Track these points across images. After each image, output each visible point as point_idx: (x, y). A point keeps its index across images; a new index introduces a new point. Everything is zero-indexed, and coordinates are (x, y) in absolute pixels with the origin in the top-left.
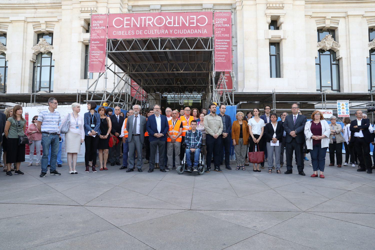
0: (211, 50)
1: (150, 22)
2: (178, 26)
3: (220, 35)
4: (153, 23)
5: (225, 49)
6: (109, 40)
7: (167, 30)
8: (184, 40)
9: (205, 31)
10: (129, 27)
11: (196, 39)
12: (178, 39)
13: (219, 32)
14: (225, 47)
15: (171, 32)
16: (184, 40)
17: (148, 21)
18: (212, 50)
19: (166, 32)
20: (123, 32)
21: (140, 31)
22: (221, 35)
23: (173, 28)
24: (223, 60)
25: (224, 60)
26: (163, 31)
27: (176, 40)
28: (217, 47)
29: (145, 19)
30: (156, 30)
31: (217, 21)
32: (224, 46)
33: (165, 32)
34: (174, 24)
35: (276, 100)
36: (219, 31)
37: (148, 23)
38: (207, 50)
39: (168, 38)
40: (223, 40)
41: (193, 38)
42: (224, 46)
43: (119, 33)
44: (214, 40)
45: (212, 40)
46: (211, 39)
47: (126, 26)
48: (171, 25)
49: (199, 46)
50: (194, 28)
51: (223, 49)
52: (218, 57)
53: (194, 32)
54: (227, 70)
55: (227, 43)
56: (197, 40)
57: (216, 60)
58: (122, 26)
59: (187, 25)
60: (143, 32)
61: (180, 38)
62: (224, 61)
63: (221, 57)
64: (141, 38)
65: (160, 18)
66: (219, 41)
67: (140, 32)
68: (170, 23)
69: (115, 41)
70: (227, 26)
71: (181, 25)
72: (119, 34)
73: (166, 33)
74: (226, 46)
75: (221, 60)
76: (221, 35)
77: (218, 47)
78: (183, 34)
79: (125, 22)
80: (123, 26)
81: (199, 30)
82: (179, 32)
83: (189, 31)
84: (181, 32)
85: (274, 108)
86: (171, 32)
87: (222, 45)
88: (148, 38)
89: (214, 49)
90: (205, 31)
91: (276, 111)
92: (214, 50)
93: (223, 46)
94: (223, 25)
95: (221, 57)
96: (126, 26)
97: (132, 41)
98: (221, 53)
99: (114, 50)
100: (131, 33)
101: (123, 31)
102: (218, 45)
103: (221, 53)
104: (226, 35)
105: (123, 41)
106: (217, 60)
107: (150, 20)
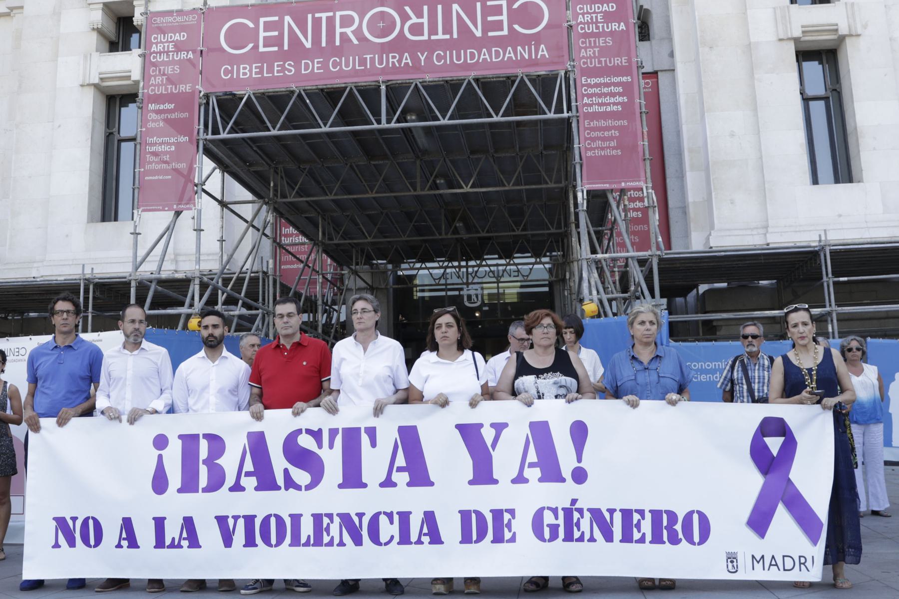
0: (565, 115)
1: (349, 31)
2: (448, 37)
3: (595, 63)
4: (358, 33)
5: (615, 108)
6: (207, 96)
7: (406, 54)
8: (469, 83)
9: (543, 51)
10: (276, 49)
11: (510, 80)
12: (447, 81)
13: (590, 52)
14: (614, 104)
15: (423, 59)
16: (469, 83)
17: (341, 27)
18: (570, 114)
19: (404, 61)
20: (256, 68)
21: (316, 61)
22: (600, 62)
23: (430, 46)
24: (609, 147)
25: (614, 148)
26: (393, 59)
27: (442, 86)
28: (586, 105)
29: (331, 21)
30: (368, 57)
31: (583, 14)
32: (612, 100)
33: (400, 61)
34: (433, 30)
35: (836, 274)
36: (590, 47)
37: (342, 34)
38: (551, 115)
39: (411, 81)
40: (607, 80)
41: (499, 77)
42: (612, 100)
43: (242, 71)
44: (575, 80)
45: (567, 79)
46: (565, 77)
47: (265, 46)
48: (422, 35)
49: (522, 104)
50: (501, 42)
51: (609, 109)
52: (593, 140)
53: (504, 55)
54: (626, 182)
55: (620, 89)
56: (513, 82)
57: (587, 149)
58: (251, 45)
59: (478, 34)
60: (324, 65)
61: (455, 78)
62: (614, 152)
63: (604, 139)
64: (321, 87)
65: (382, 13)
66: (593, 81)
67: (316, 65)
68: (416, 29)
69: (226, 99)
70: (619, 27)
71: (455, 36)
72: (241, 77)
73: (407, 64)
74: (620, 99)
75: (603, 149)
76: (600, 62)
77: (591, 105)
78: (466, 66)
79: (262, 34)
80: (256, 47)
81: (519, 48)
82: (452, 58)
83: (485, 55)
84: (459, 59)
85: (830, 305)
86: (423, 59)
87: (605, 95)
88: (343, 85)
89: (577, 111)
90: (543, 51)
91: (838, 314)
92: (578, 117)
93: (608, 100)
94: (603, 27)
95: (604, 139)
96: (265, 46)
97: (287, 95)
98: (603, 123)
99: (224, 131)
100: (283, 69)
101: (254, 65)
102: (590, 96)
103: (603, 123)
104: (617, 61)
105: (256, 97)
106: (591, 149)
107: (347, 21)
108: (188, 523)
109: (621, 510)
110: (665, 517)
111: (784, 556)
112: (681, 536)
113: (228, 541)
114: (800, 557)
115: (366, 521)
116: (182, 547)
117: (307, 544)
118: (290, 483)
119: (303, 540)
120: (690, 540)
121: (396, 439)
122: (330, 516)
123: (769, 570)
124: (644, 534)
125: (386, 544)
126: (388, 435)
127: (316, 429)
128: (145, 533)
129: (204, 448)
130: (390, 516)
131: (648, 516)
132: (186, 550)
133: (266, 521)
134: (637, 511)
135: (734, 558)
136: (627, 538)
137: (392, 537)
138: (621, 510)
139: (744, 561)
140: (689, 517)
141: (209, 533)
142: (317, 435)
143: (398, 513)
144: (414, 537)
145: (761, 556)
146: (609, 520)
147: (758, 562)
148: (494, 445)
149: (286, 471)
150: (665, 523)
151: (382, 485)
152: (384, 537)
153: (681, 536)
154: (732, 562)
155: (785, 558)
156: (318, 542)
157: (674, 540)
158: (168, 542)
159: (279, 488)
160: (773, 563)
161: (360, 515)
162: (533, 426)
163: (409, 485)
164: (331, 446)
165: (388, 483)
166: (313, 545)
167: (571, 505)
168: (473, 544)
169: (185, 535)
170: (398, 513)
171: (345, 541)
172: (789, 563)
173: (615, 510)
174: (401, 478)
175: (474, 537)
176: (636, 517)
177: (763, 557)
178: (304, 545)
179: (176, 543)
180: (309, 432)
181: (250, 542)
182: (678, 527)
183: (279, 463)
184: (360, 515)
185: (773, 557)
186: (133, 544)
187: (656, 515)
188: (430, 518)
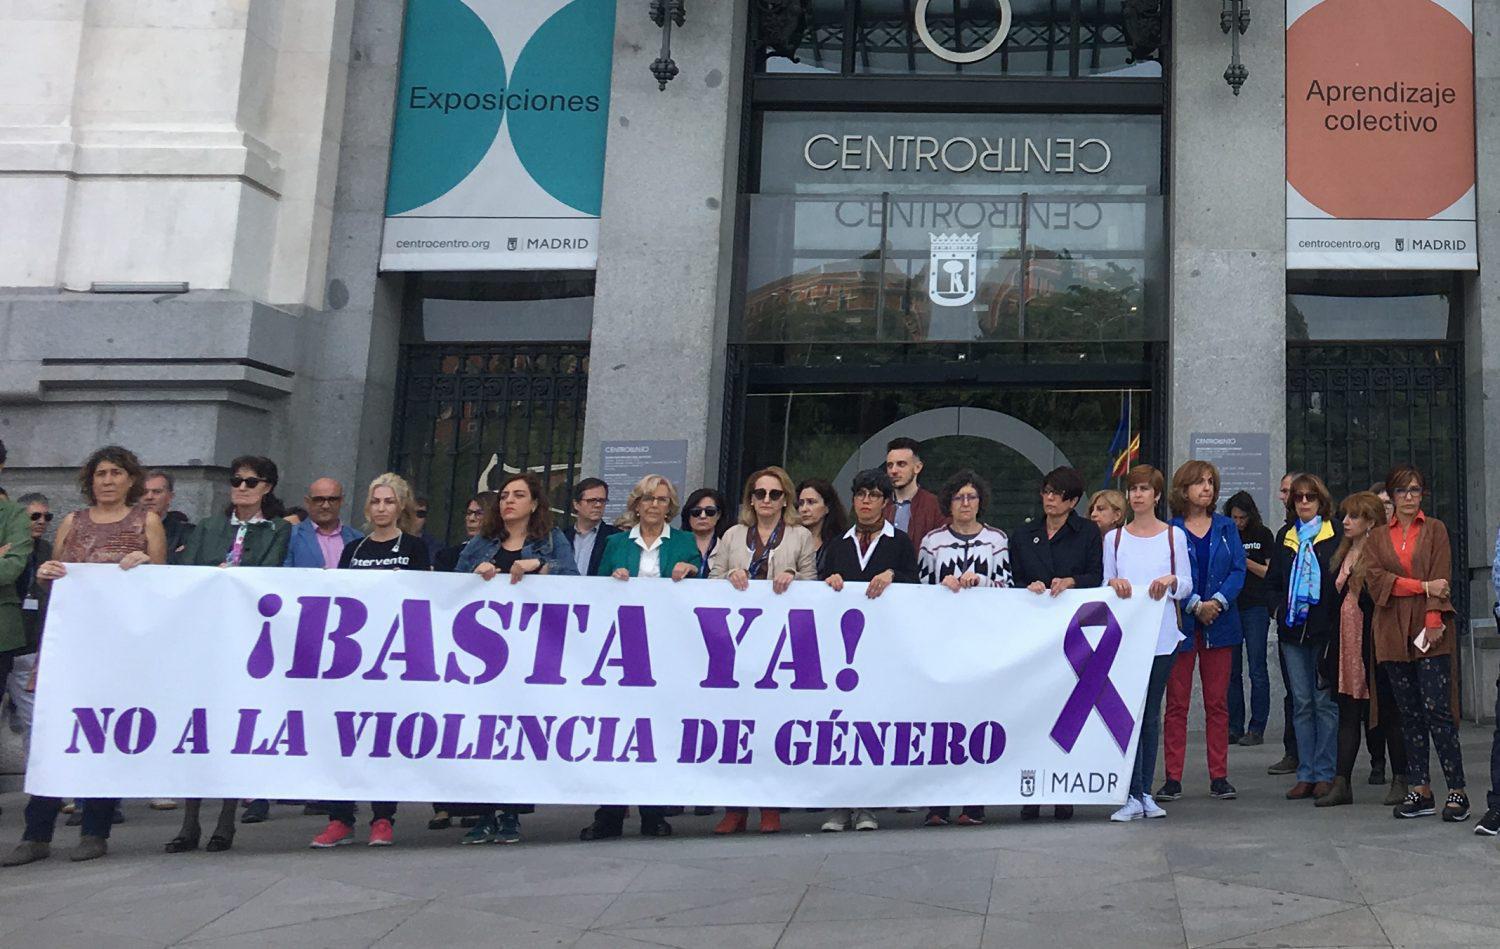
108: (295, 720)
109: (897, 724)
110: (950, 730)
111: (1091, 774)
112: (967, 753)
113: (348, 745)
114: (1110, 775)
115: (556, 727)
116: (276, 753)
117: (466, 755)
118: (454, 672)
119: (461, 749)
120: (978, 758)
121: (614, 624)
122: (507, 720)
123: (1072, 790)
124: (922, 754)
125: (579, 759)
126: (603, 618)
127: (504, 603)
128: (222, 731)
129: (333, 619)
130: (589, 722)
131: (930, 730)
132: (283, 758)
133: (409, 722)
134: (916, 725)
135: (1031, 778)
136: (901, 758)
137: (588, 751)
138: (897, 724)
139: (1042, 781)
140: (980, 730)
141: (321, 733)
142: (504, 611)
143: (601, 719)
144: (617, 752)
145: (1052, 776)
146: (879, 737)
147: (1060, 782)
148: (740, 638)
149: (452, 657)
150: (949, 738)
151: (586, 682)
152: (575, 752)
153: (967, 753)
154: (1028, 783)
155: (1093, 777)
156: (484, 751)
157: (958, 758)
158: (256, 744)
159: (436, 678)
160: (1078, 782)
161: (550, 720)
162: (795, 616)
163: (622, 683)
164: (523, 626)
165: (595, 679)
166: (476, 757)
167: (831, 718)
168: (695, 764)
169: (285, 736)
170: (601, 719)
171: (523, 752)
172: (1096, 782)
173: (889, 724)
174: (613, 674)
175: (698, 755)
176: (915, 732)
177: (1066, 776)
178: (461, 756)
179: (269, 747)
180: (494, 605)
181: (380, 750)
182: (965, 743)
183: (443, 643)
184: (550, 720)
185: (1079, 775)
186: (200, 746)
187: (940, 729)
188: (643, 727)
